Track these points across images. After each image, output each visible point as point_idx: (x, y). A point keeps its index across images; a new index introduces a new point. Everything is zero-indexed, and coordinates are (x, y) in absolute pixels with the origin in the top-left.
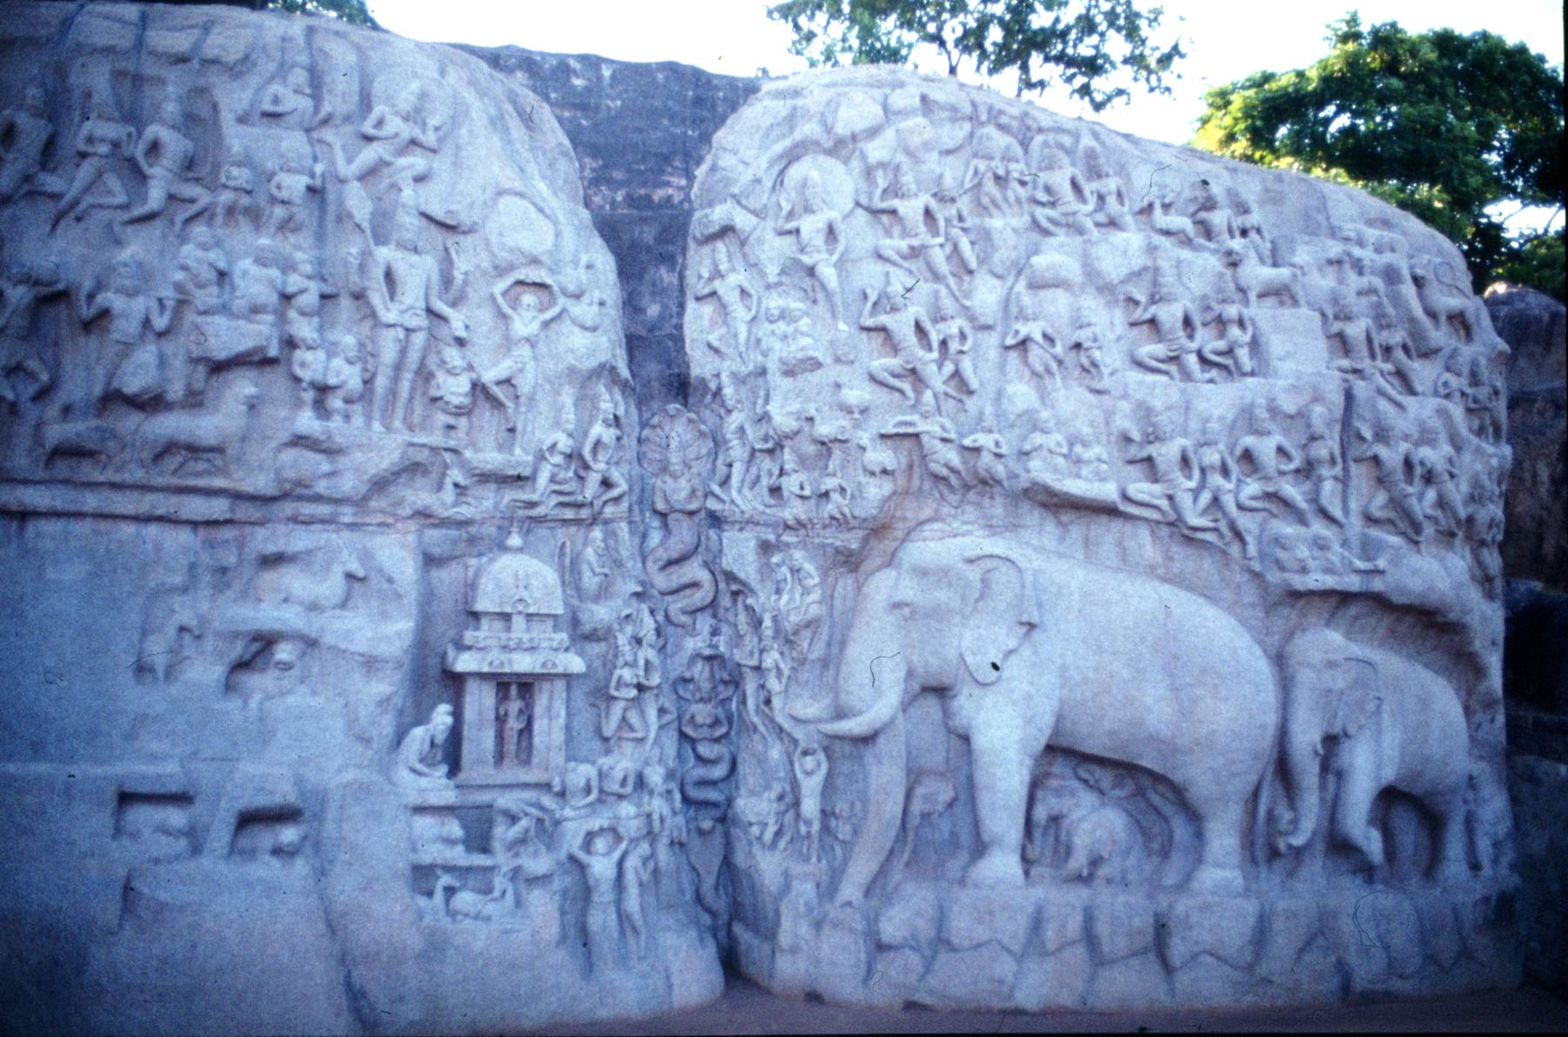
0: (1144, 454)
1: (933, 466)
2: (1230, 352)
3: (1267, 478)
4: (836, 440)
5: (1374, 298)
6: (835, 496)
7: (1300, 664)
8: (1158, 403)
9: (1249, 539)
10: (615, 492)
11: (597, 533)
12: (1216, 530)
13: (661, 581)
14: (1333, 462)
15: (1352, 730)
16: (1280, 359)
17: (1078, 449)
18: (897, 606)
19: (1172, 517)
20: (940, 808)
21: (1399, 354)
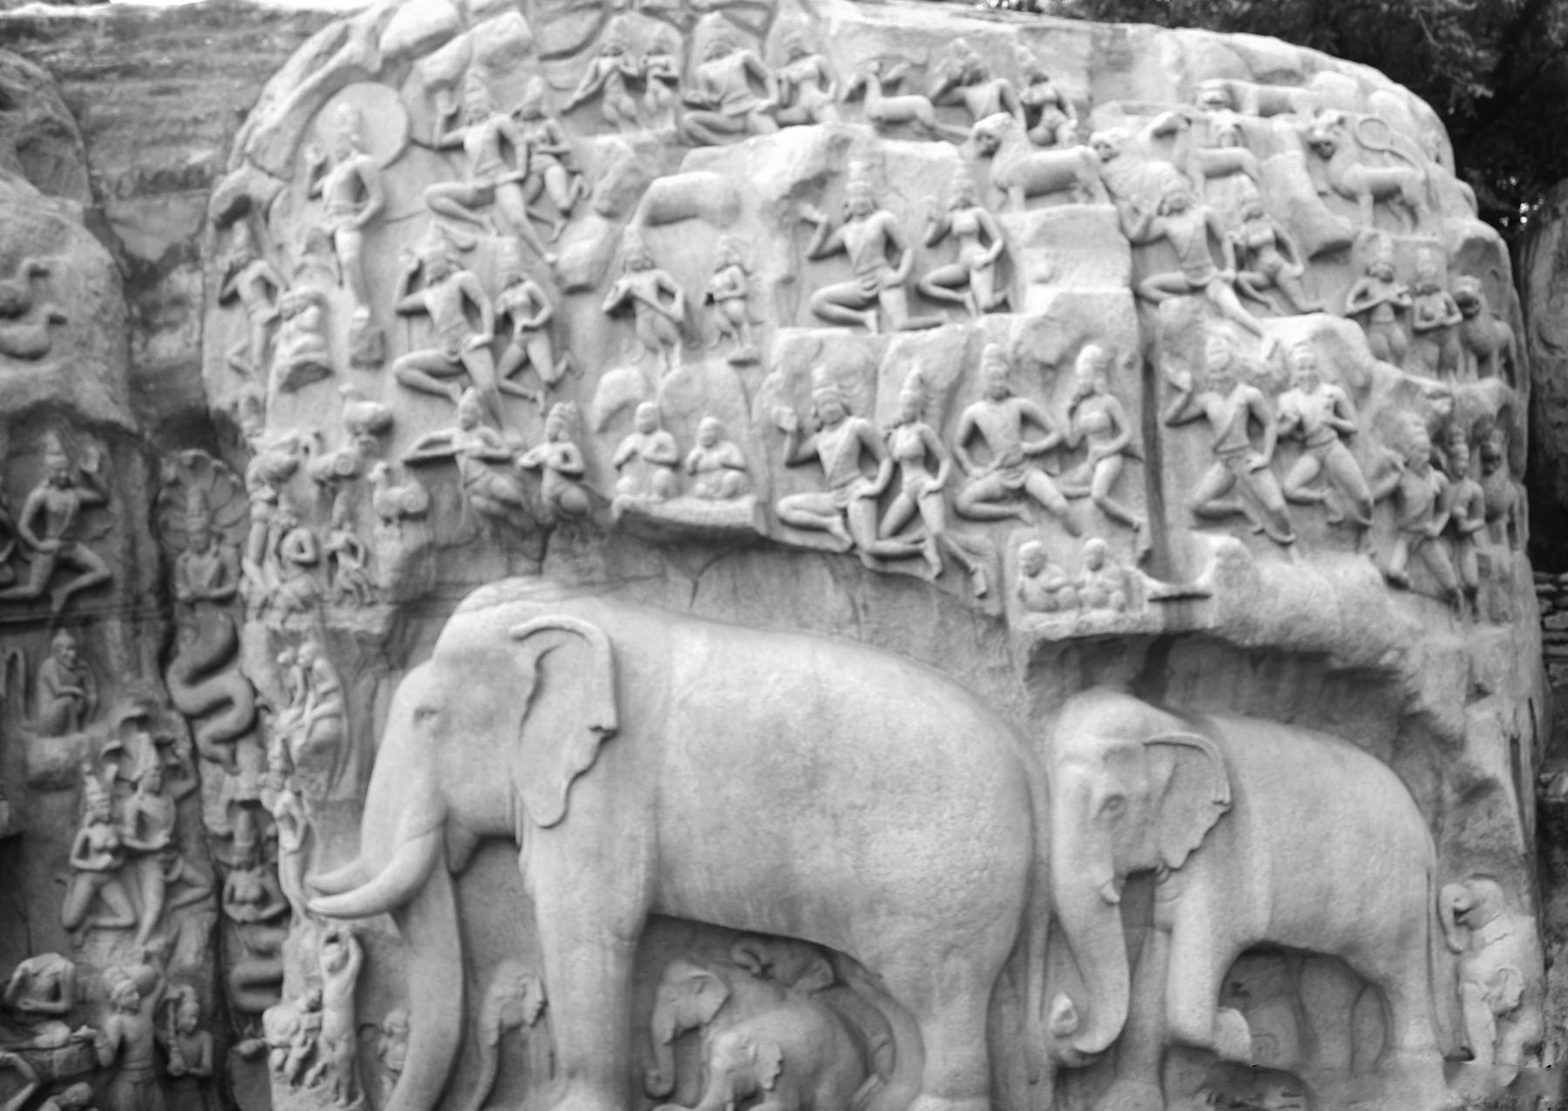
0: (806, 449)
1: (479, 501)
2: (962, 283)
3: (1009, 467)
4: (336, 478)
5: (1234, 180)
6: (344, 560)
7: (1071, 758)
8: (819, 373)
9: (973, 564)
10: (85, 580)
11: (63, 639)
12: (916, 556)
13: (190, 698)
14: (1113, 428)
15: (1176, 859)
16: (1043, 281)
17: (692, 455)
18: (421, 714)
19: (848, 540)
20: (529, 1015)
21: (1271, 257)
